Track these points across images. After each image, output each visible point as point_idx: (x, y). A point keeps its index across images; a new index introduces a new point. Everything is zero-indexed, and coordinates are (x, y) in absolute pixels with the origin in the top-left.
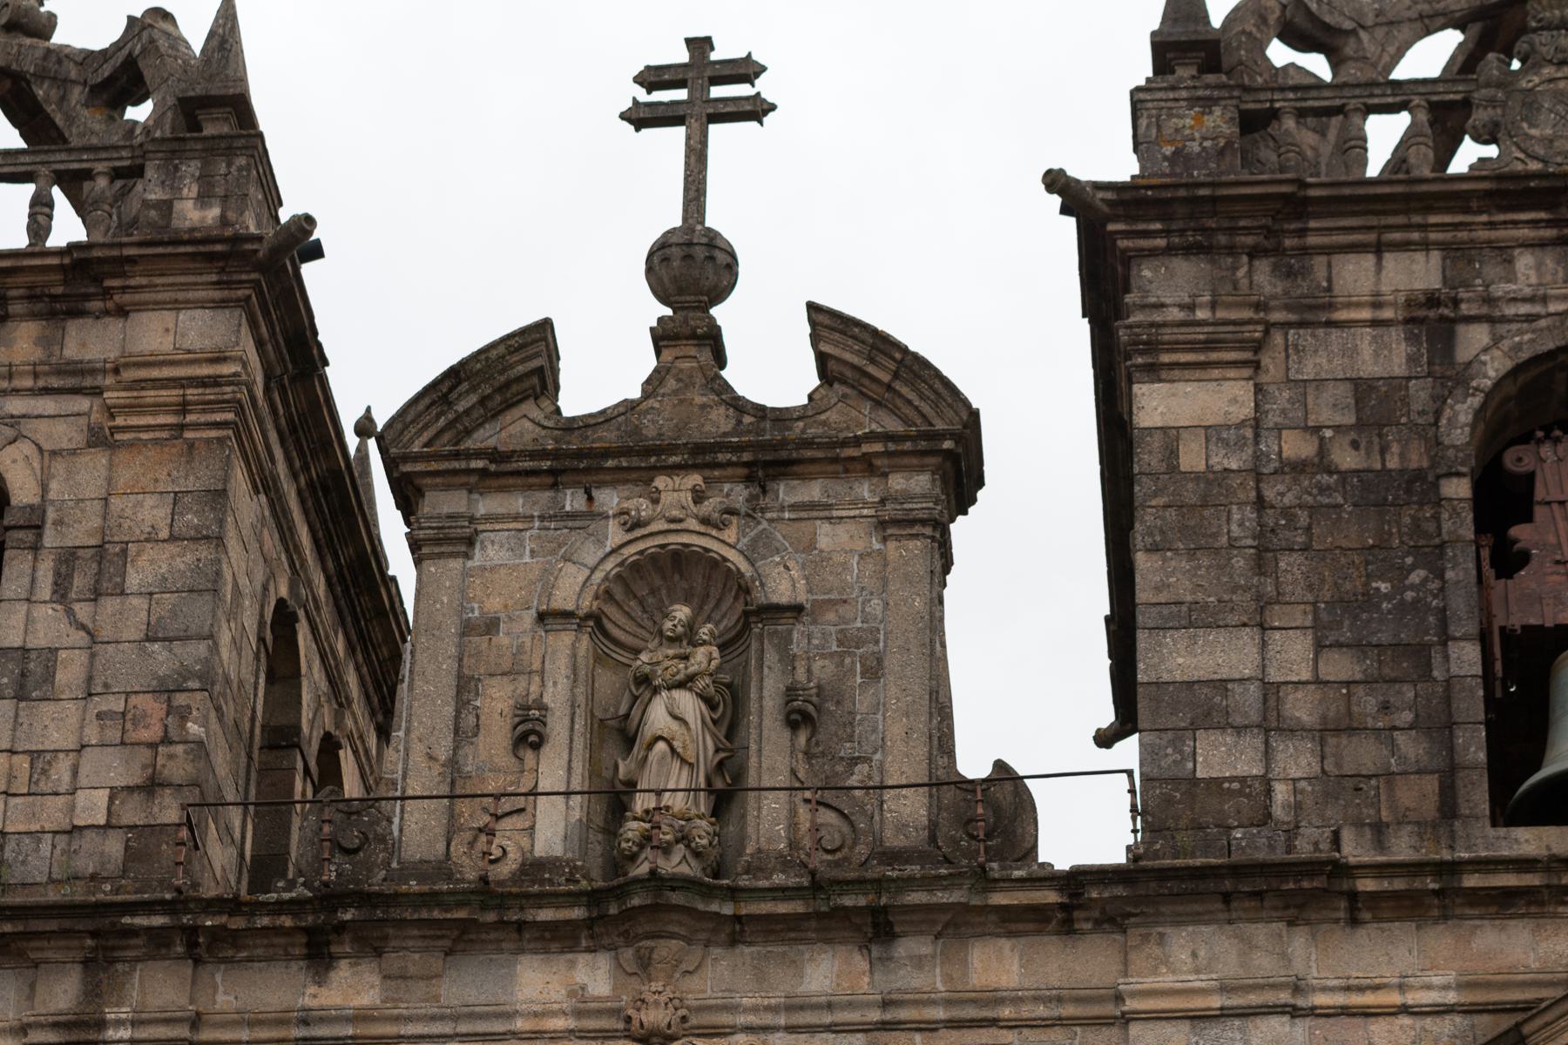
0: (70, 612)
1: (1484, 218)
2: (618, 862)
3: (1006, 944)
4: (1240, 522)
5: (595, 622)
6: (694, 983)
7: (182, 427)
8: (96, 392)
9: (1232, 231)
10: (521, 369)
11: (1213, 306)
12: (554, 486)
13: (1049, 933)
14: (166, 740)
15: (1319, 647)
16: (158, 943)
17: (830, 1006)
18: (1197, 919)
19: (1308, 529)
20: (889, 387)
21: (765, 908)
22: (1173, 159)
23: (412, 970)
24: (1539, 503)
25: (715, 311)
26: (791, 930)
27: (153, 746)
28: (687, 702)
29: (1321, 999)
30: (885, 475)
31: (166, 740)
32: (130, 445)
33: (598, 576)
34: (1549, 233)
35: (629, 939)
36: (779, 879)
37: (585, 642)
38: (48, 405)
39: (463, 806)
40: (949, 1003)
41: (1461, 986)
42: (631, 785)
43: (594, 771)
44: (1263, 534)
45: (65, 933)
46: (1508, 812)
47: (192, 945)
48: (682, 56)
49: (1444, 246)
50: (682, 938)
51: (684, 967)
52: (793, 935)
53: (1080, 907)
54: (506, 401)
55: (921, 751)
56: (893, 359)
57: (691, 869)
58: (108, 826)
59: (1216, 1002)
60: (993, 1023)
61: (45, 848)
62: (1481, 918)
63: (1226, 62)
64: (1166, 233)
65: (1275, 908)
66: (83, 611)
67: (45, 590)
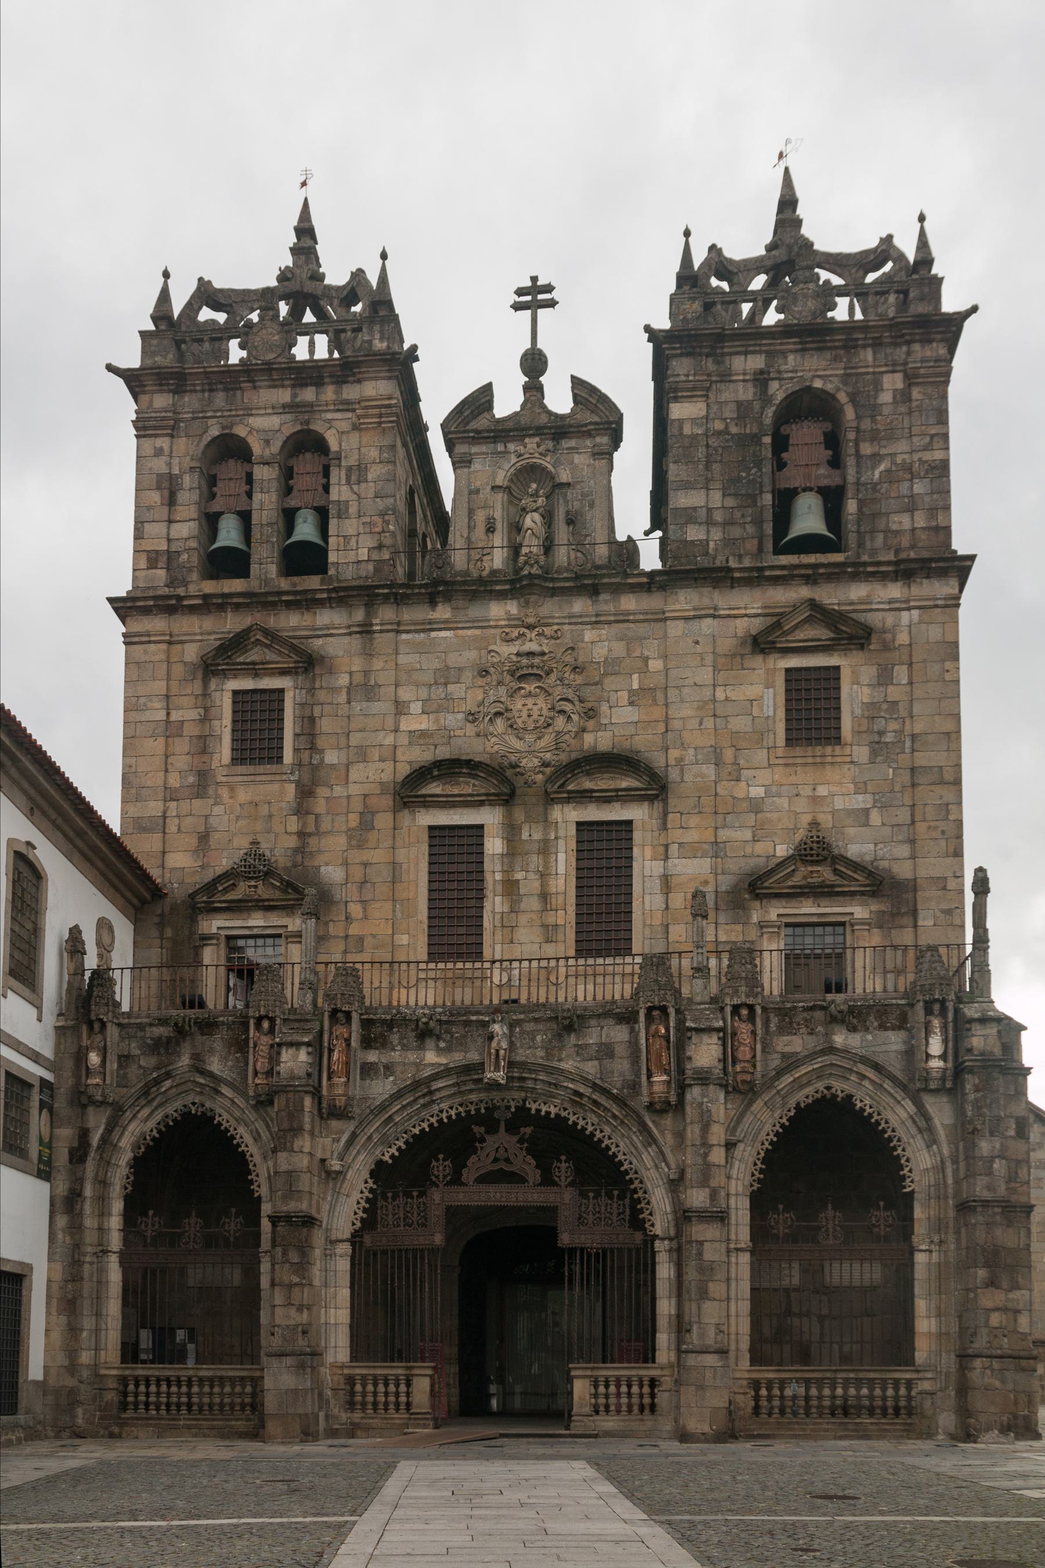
0: (351, 488)
2: (517, 571)
3: (631, 595)
6: (541, 609)
7: (380, 423)
11: (695, 375)
12: (494, 442)
14: (383, 531)
16: (386, 597)
17: (581, 616)
18: (687, 587)
21: (561, 584)
22: (683, 321)
23: (461, 606)
25: (541, 379)
27: (379, 533)
29: (722, 612)
31: (383, 531)
32: (366, 429)
35: (522, 595)
36: (565, 575)
37: (506, 497)
39: (472, 552)
40: (615, 615)
42: (521, 545)
43: (509, 541)
45: (359, 595)
46: (778, 551)
47: (396, 599)
55: (606, 532)
57: (539, 572)
58: (368, 560)
59: (692, 613)
60: (628, 621)
61: (350, 568)
63: (699, 283)
66: (355, 488)
67: (343, 482)
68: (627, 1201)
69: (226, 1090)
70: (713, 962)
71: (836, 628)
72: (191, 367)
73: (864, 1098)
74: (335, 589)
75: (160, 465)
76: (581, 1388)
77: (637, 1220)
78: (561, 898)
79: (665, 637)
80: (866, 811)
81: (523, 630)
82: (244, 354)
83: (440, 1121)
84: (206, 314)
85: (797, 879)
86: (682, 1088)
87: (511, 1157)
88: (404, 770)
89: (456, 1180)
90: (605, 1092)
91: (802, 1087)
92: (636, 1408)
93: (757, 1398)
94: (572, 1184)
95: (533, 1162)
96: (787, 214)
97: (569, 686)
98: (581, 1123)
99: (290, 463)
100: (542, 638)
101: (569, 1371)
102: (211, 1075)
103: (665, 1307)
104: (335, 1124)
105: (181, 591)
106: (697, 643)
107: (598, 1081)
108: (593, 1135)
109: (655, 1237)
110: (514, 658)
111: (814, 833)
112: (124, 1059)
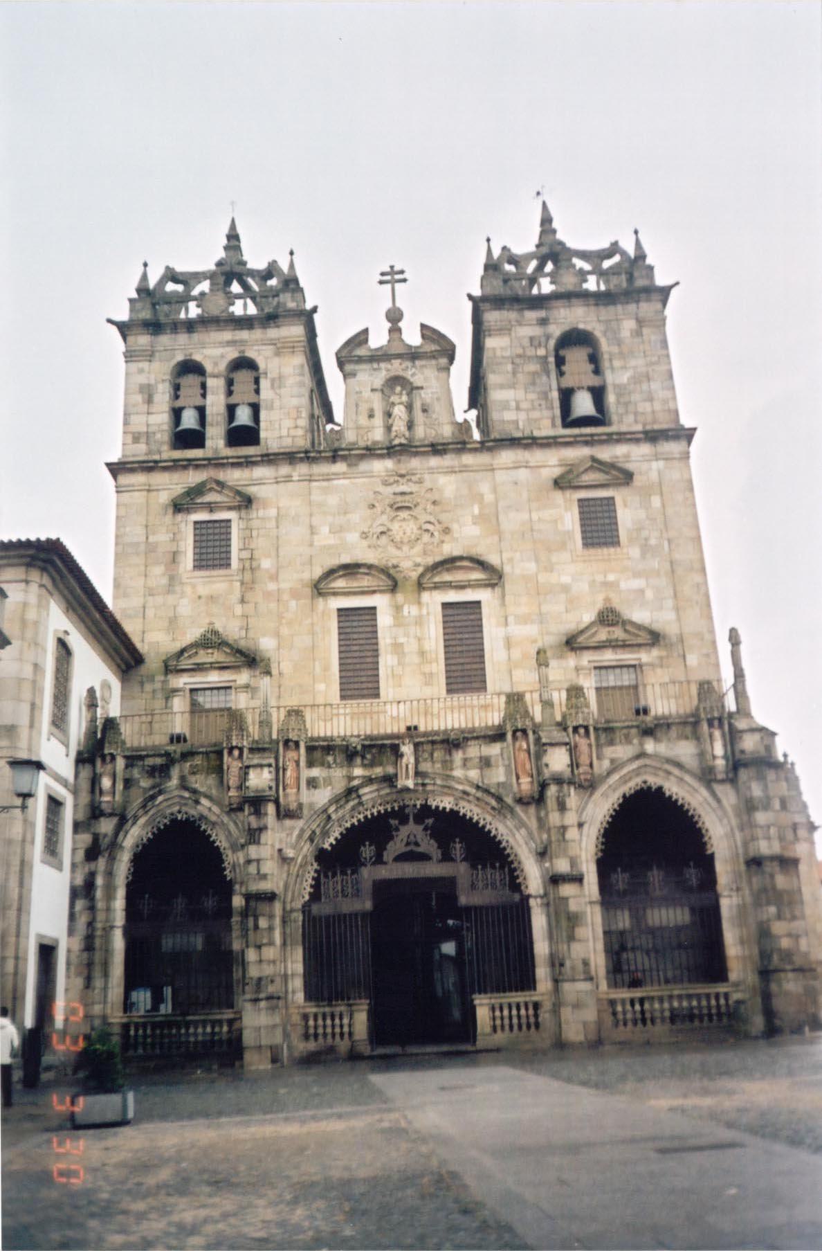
4: (509, 367)
5: (382, 391)
8: (275, 344)
16: (302, 460)
28: (402, 408)
38: (264, 347)
42: (392, 425)
44: (514, 369)
48: (388, 269)
66: (278, 391)
68: (506, 869)
69: (204, 801)
70: (555, 696)
72: (163, 319)
73: (673, 789)
74: (267, 455)
75: (142, 379)
76: (483, 1014)
77: (514, 882)
78: (434, 656)
79: (494, 479)
80: (642, 591)
81: (396, 478)
82: (199, 311)
83: (366, 817)
84: (171, 287)
85: (597, 639)
86: (543, 786)
87: (419, 840)
88: (318, 572)
89: (379, 860)
90: (487, 791)
91: (626, 782)
92: (524, 1027)
93: (614, 1014)
94: (464, 860)
95: (436, 845)
96: (547, 226)
97: (431, 514)
98: (469, 815)
99: (231, 376)
100: (410, 484)
101: (472, 1000)
102: (195, 792)
103: (541, 947)
104: (288, 823)
105: (157, 457)
106: (516, 483)
107: (480, 784)
108: (478, 823)
109: (529, 896)
110: (392, 496)
111: (608, 605)
112: (128, 783)
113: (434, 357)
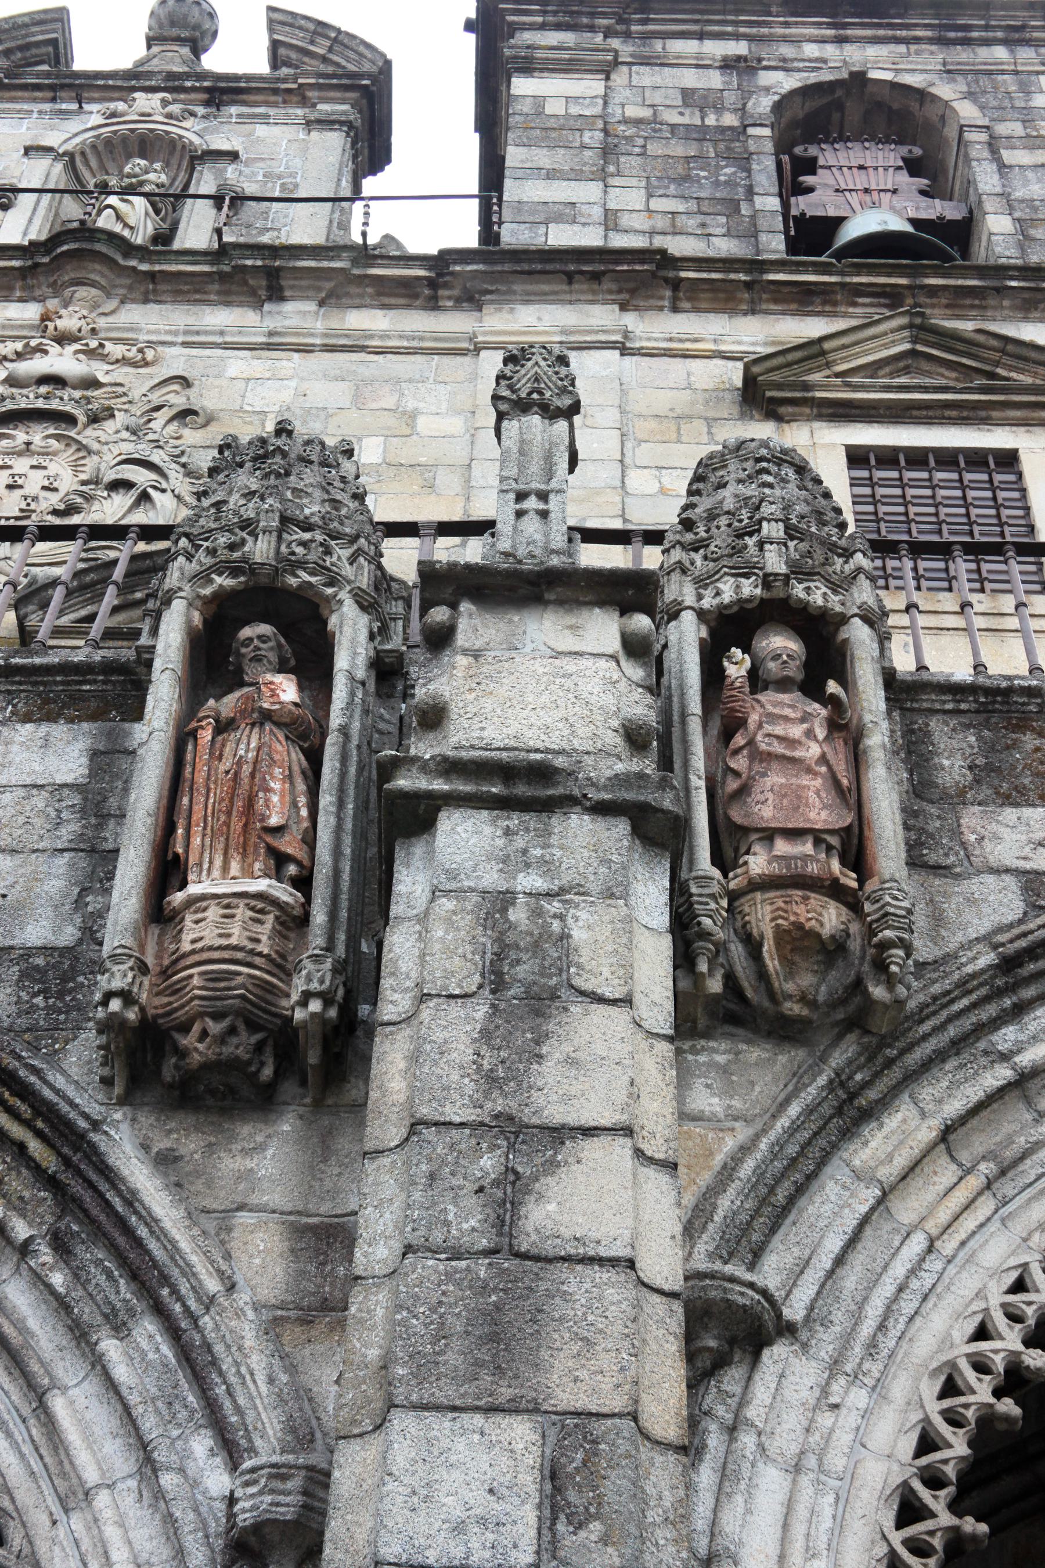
1: (781, 19)
3: (379, 313)
9: (593, 15)
10: (40, 38)
13: (416, 308)
15: (650, 196)
17: (222, 333)
19: (644, 146)
20: (324, 59)
24: (821, 167)
26: (197, 291)
30: (314, 105)
33: (78, 140)
34: (831, 32)
35: (57, 289)
40: (326, 335)
41: (766, 344)
49: (750, 38)
50: (102, 288)
51: (101, 310)
52: (198, 297)
53: (446, 286)
54: (25, 58)
56: (328, 37)
60: (362, 349)
62: (784, 313)
64: (544, 13)
65: (610, 292)
71: (992, 376)
113: (299, 96)
